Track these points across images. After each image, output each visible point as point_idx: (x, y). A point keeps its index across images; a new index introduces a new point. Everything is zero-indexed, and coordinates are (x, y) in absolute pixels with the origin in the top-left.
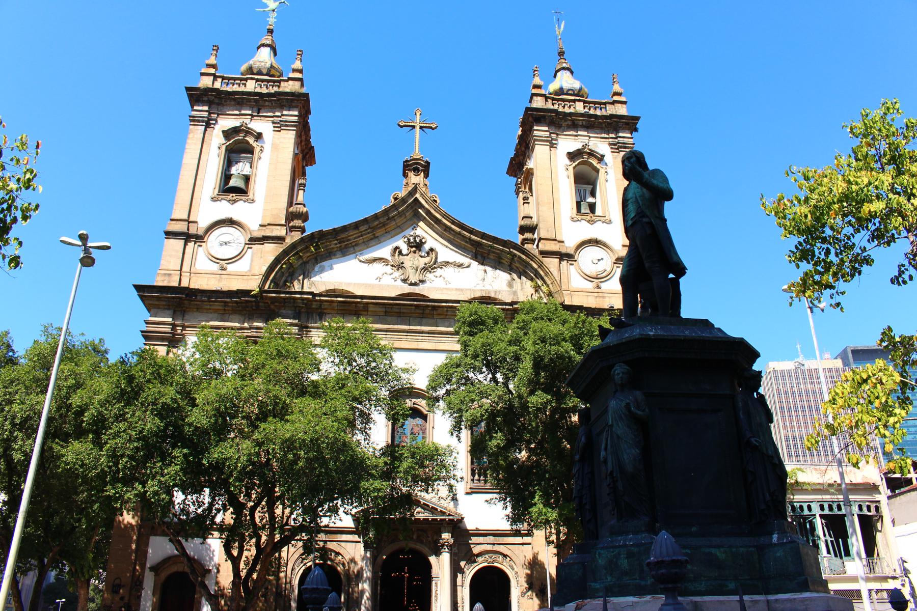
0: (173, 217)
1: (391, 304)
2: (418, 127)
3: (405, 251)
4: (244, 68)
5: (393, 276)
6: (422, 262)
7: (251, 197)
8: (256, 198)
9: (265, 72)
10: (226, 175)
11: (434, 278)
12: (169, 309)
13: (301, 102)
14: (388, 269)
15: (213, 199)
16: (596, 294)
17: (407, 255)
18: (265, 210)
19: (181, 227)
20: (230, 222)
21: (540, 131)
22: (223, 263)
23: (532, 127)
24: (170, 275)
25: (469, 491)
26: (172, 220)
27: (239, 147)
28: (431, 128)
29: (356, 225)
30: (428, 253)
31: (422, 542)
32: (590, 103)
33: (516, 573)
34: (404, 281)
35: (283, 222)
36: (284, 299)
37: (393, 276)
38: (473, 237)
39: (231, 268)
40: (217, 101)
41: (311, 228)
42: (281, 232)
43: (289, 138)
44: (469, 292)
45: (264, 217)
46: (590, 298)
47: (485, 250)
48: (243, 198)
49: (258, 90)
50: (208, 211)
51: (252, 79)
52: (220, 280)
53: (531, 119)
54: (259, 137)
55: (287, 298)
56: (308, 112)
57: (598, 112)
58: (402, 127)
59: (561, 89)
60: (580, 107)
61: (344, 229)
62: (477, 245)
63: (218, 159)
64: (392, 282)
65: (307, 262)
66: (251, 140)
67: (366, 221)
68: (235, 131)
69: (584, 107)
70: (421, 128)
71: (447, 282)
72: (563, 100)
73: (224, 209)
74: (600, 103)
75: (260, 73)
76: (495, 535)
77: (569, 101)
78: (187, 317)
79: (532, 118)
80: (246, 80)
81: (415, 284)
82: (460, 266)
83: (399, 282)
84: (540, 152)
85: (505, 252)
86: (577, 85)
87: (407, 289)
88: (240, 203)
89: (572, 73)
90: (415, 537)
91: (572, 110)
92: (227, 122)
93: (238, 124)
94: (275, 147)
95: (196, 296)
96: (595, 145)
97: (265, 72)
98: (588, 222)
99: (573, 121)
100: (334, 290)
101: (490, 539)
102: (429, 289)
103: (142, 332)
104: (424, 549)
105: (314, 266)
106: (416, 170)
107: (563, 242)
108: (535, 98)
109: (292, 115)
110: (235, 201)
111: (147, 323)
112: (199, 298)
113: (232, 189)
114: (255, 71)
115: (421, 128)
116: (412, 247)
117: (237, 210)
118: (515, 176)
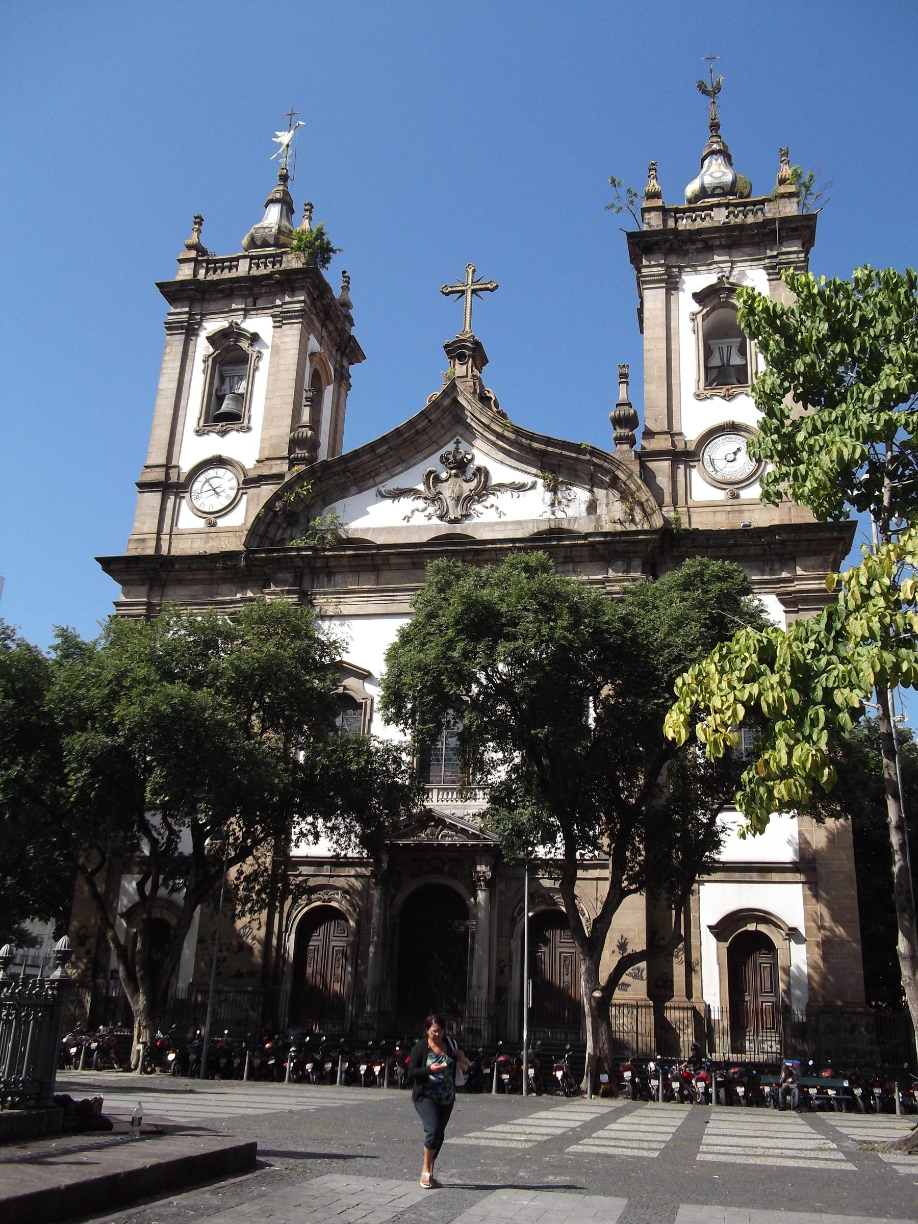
0: (149, 463)
1: (417, 553)
2: (469, 292)
3: (444, 475)
4: (245, 241)
5: (427, 513)
6: (467, 488)
8: (252, 424)
9: (271, 241)
12: (144, 585)
13: (308, 279)
14: (420, 504)
15: (199, 433)
16: (729, 508)
17: (447, 480)
18: (262, 440)
19: (157, 475)
20: (219, 462)
22: (212, 517)
24: (143, 540)
26: (147, 467)
27: (231, 356)
28: (487, 289)
30: (474, 474)
34: (441, 517)
35: (286, 454)
36: (278, 559)
37: (427, 513)
38: (536, 445)
39: (222, 523)
42: (283, 467)
46: (718, 514)
47: (557, 462)
48: (235, 427)
50: (193, 449)
52: (206, 542)
54: (254, 338)
55: (283, 557)
58: (447, 294)
62: (544, 453)
63: (203, 376)
65: (313, 505)
66: (244, 344)
67: (384, 440)
78: (165, 591)
81: (456, 521)
82: (520, 488)
83: (435, 521)
85: (583, 461)
87: (444, 528)
88: (234, 433)
90: (446, 869)
92: (213, 325)
93: (226, 324)
94: (276, 350)
95: (174, 565)
97: (271, 241)
98: (723, 397)
99: (705, 241)
104: (460, 888)
105: (322, 509)
108: (647, 215)
111: (117, 604)
112: (177, 566)
113: (223, 416)
114: (259, 243)
116: (451, 469)
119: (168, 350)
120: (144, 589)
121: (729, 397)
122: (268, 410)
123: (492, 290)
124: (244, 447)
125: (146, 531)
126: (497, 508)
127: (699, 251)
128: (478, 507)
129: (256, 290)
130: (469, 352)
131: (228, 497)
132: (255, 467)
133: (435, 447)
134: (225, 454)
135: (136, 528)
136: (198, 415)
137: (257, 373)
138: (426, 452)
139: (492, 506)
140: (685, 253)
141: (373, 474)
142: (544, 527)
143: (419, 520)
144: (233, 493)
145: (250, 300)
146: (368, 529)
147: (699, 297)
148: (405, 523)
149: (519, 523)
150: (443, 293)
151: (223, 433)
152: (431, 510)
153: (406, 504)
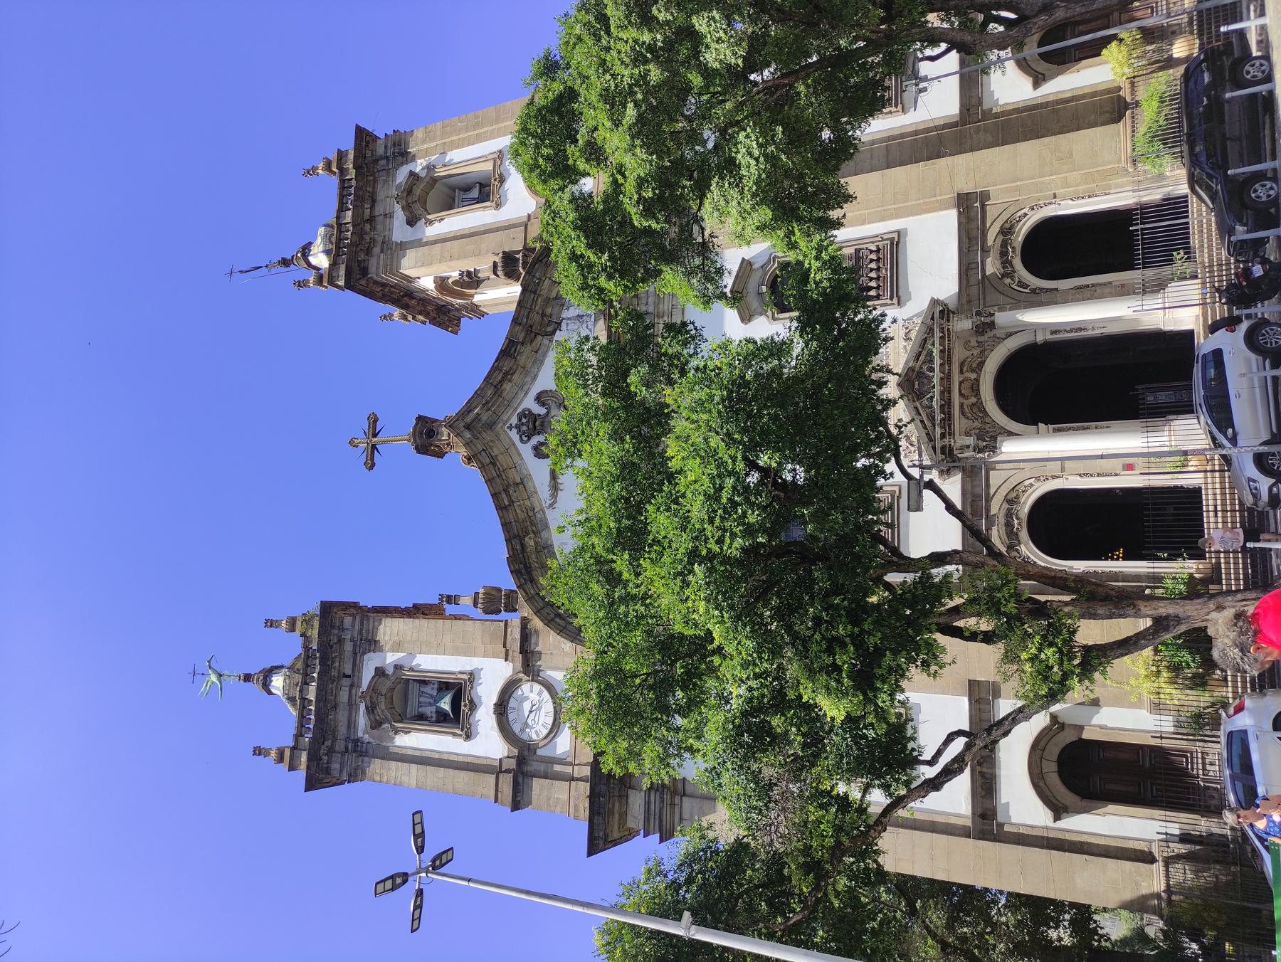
7: (464, 677)
10: (438, 721)
19: (507, 782)
20: (501, 708)
25: (895, 300)
29: (501, 508)
30: (543, 404)
40: (328, 743)
43: (389, 629)
45: (495, 656)
50: (488, 743)
53: (363, 282)
54: (380, 672)
56: (355, 605)
61: (506, 526)
63: (413, 734)
66: (385, 686)
68: (371, 710)
70: (375, 435)
73: (485, 718)
86: (322, 230)
93: (362, 707)
96: (398, 187)
103: (661, 841)
110: (472, 702)
118: (459, 319)
119: (378, 778)
120: (631, 793)
122: (456, 652)
123: (376, 421)
125: (567, 797)
127: (373, 228)
129: (334, 673)
130: (426, 437)
131: (540, 694)
132: (513, 661)
133: (512, 451)
134: (494, 699)
135: (562, 804)
136: (450, 738)
138: (516, 459)
140: (373, 240)
141: (531, 513)
144: (537, 687)
145: (346, 682)
150: (371, 468)
151: (473, 706)
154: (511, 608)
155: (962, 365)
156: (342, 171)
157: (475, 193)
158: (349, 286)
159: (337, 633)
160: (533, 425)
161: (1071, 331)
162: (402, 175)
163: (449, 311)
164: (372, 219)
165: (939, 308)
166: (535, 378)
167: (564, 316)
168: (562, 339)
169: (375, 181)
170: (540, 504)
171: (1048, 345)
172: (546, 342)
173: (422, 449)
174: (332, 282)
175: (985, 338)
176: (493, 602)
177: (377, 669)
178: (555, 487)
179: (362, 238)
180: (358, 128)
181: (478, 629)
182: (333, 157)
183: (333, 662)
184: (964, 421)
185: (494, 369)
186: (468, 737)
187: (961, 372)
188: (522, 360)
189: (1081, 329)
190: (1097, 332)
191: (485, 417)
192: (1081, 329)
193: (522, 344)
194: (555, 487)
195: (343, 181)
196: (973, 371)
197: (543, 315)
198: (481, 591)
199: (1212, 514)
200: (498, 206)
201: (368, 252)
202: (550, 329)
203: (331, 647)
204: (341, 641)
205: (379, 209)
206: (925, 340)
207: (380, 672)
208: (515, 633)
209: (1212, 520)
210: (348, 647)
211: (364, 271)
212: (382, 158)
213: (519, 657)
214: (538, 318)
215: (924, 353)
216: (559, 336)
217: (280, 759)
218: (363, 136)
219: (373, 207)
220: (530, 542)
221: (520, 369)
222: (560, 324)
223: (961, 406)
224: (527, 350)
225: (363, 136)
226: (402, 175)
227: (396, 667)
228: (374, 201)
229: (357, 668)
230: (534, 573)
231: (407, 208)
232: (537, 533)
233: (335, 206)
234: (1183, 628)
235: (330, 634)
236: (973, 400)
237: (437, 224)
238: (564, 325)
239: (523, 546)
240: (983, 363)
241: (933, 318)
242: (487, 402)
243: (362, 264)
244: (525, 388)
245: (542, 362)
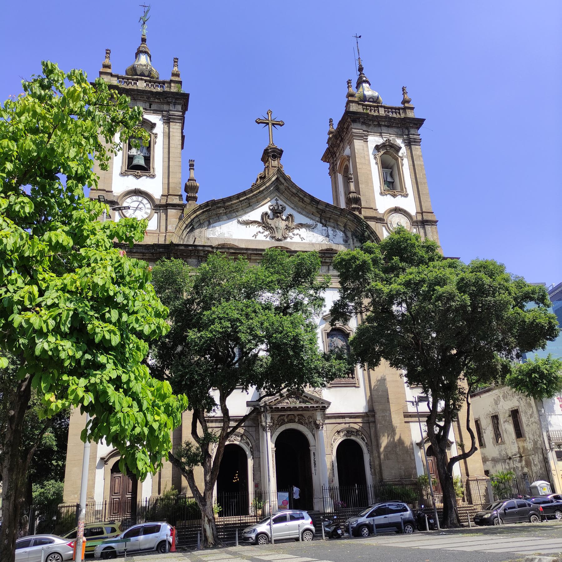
3: (271, 217)
8: (156, 173)
9: (146, 73)
11: (293, 236)
13: (182, 100)
14: (260, 229)
15: (123, 174)
20: (137, 192)
21: (356, 129)
23: (348, 126)
29: (238, 196)
30: (288, 218)
31: (302, 424)
32: (388, 108)
33: (366, 443)
34: (273, 237)
41: (203, 198)
44: (318, 246)
48: (147, 174)
49: (148, 89)
51: (142, 79)
53: (349, 120)
54: (153, 125)
57: (394, 115)
59: (364, 96)
60: (382, 112)
61: (230, 199)
64: (264, 239)
69: (385, 111)
70: (273, 124)
71: (302, 239)
72: (370, 106)
74: (395, 109)
75: (142, 74)
76: (351, 417)
77: (374, 107)
79: (350, 118)
80: (137, 80)
84: (358, 144)
86: (376, 94)
88: (144, 178)
89: (370, 85)
91: (376, 114)
97: (146, 73)
100: (224, 245)
101: (347, 420)
102: (291, 243)
106: (274, 157)
107: (377, 210)
108: (351, 104)
109: (176, 112)
110: (140, 176)
114: (139, 73)
115: (273, 124)
117: (144, 183)
121: (394, 196)
123: (281, 126)
124: (154, 186)
126: (300, 235)
127: (375, 126)
128: (291, 234)
129: (152, 99)
130: (272, 153)
131: (146, 213)
134: (143, 189)
137: (156, 146)
139: (297, 234)
140: (369, 125)
142: (325, 247)
143: (261, 237)
145: (147, 105)
146: (235, 240)
147: (377, 148)
148: (254, 238)
149: (313, 244)
151: (138, 177)
152: (267, 233)
153: (255, 229)
154: (188, 199)
155: (301, 415)
156: (405, 109)
157: (389, 179)
158: (348, 113)
159: (172, 101)
160: (277, 212)
161: (315, 461)
162: (399, 142)
163: (333, 158)
164: (379, 125)
165: (326, 406)
166: (300, 213)
167: (329, 228)
168: (318, 226)
169: (398, 127)
170: (240, 215)
171: (309, 451)
172: (317, 219)
173: (266, 152)
174: (349, 102)
175: (313, 425)
176: (191, 189)
177: (155, 124)
178: (247, 223)
179: (370, 120)
180: (423, 120)
181: (178, 182)
182: (411, 105)
183: (158, 99)
184: (277, 417)
185: (306, 194)
186: (123, 174)
187: (298, 415)
188: (309, 207)
189: (315, 465)
190: (313, 471)
191: (282, 187)
192: (315, 465)
193: (317, 208)
194: (247, 223)
195: (399, 109)
196: (299, 420)
197: (330, 218)
198: (198, 184)
199: (239, 519)
200: (381, 194)
201: (363, 123)
202: (323, 221)
203: (166, 98)
204: (168, 103)
205: (384, 129)
206: (313, 400)
207: (153, 125)
208: (176, 201)
209: (235, 519)
210: (165, 107)
211: (354, 121)
212: (409, 132)
213: (163, 202)
214: (328, 216)
215: (307, 399)
216: (320, 225)
217: (105, 66)
218: (418, 123)
219: (385, 126)
220: (221, 211)
221: (305, 206)
222: (325, 226)
223: (284, 415)
224: (314, 210)
225: (418, 123)
226: (399, 142)
227: (156, 134)
228: (388, 126)
229: (156, 112)
230: (207, 213)
231: (384, 146)
232: (226, 214)
233: (388, 105)
234: (201, 507)
235: (172, 98)
236: (286, 420)
237: (375, 161)
238: (324, 228)
239: (220, 207)
240: (302, 424)
241: (322, 403)
242: (289, 189)
243: (359, 117)
244: (295, 208)
245: (308, 217)
